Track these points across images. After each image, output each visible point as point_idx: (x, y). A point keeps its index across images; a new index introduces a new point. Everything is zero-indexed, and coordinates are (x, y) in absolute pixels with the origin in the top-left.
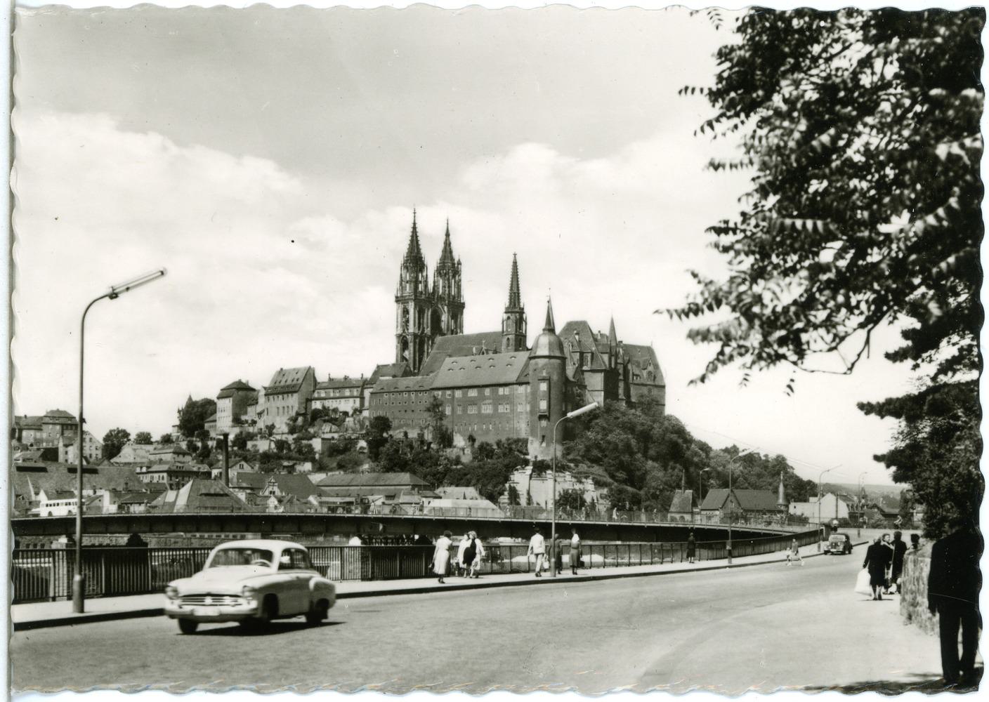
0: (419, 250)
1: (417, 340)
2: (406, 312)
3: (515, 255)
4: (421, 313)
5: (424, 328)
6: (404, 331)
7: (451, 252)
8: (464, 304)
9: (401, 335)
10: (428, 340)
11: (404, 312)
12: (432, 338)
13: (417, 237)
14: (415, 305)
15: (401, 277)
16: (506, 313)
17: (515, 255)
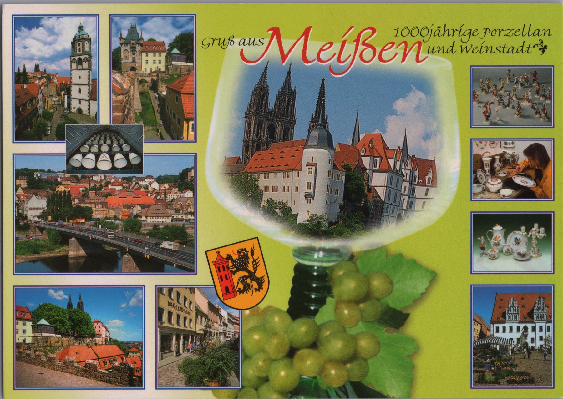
0: (265, 82)
1: (255, 145)
2: (250, 124)
3: (323, 80)
4: (260, 126)
5: (261, 136)
6: (248, 138)
7: (289, 84)
8: (295, 121)
9: (246, 141)
10: (264, 146)
11: (249, 124)
12: (267, 144)
13: (266, 74)
14: (256, 119)
15: (251, 101)
16: (312, 122)
17: (323, 80)
